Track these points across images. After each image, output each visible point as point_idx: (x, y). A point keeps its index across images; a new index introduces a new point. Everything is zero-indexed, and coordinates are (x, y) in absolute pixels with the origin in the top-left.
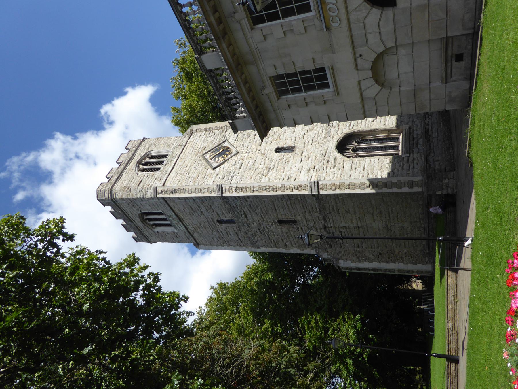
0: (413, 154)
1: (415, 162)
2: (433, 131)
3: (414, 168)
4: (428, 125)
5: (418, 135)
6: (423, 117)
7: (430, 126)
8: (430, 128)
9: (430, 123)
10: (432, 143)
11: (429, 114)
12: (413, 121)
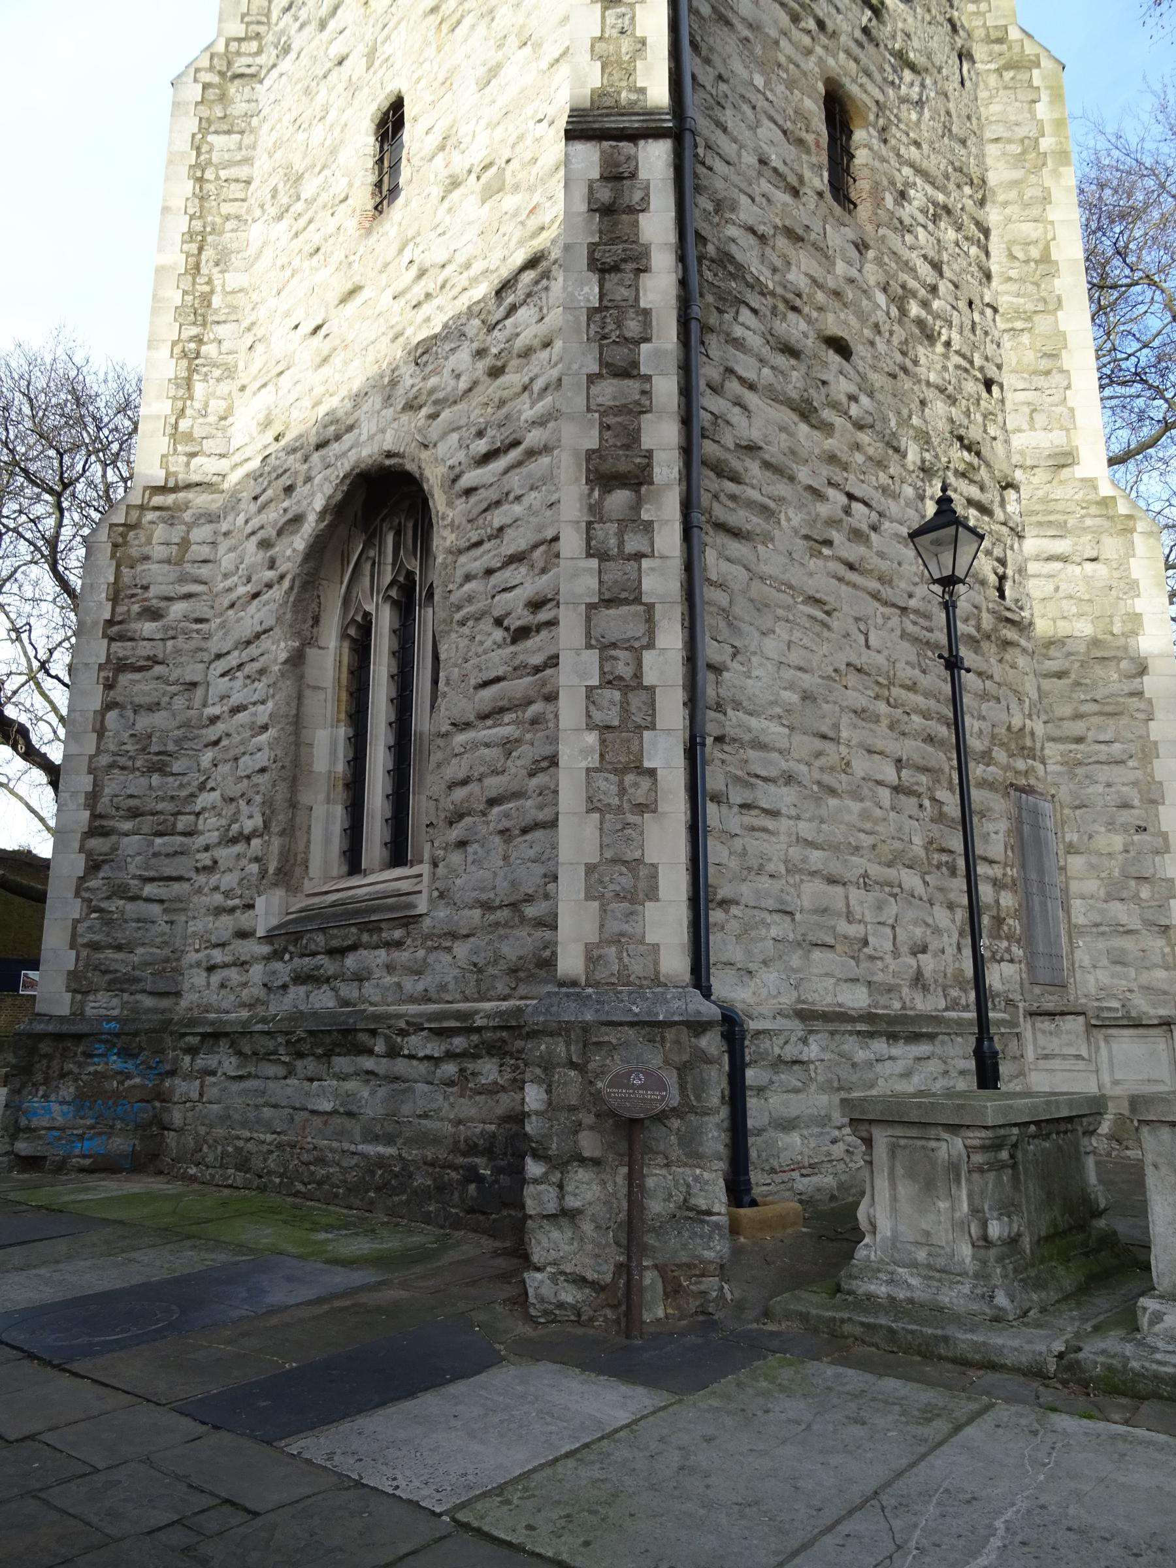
0: (267, 959)
1: (233, 974)
2: (351, 1085)
3: (211, 969)
4: (393, 1052)
5: (360, 978)
6: (459, 1015)
7: (381, 1066)
8: (368, 1063)
9: (401, 1066)
10: (280, 1071)
11: (471, 1066)
12: (454, 936)
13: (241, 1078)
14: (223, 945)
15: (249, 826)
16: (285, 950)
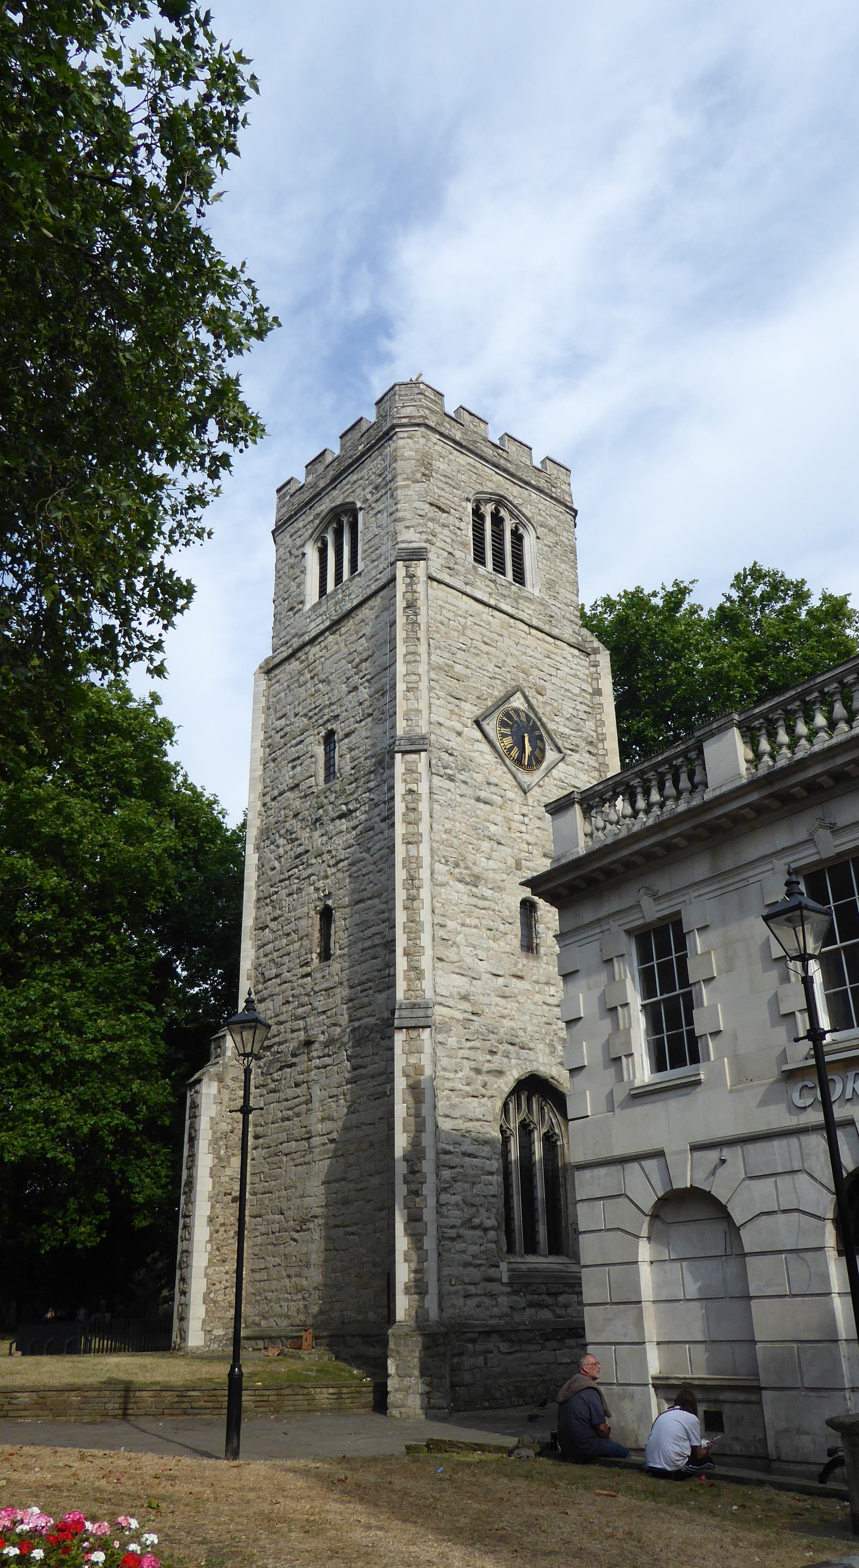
0: (509, 1294)
1: (487, 1301)
5: (566, 1306)
13: (510, 1353)
14: (475, 1284)
15: (489, 1223)
16: (520, 1291)
